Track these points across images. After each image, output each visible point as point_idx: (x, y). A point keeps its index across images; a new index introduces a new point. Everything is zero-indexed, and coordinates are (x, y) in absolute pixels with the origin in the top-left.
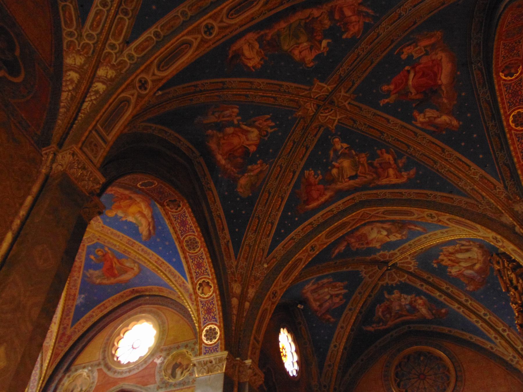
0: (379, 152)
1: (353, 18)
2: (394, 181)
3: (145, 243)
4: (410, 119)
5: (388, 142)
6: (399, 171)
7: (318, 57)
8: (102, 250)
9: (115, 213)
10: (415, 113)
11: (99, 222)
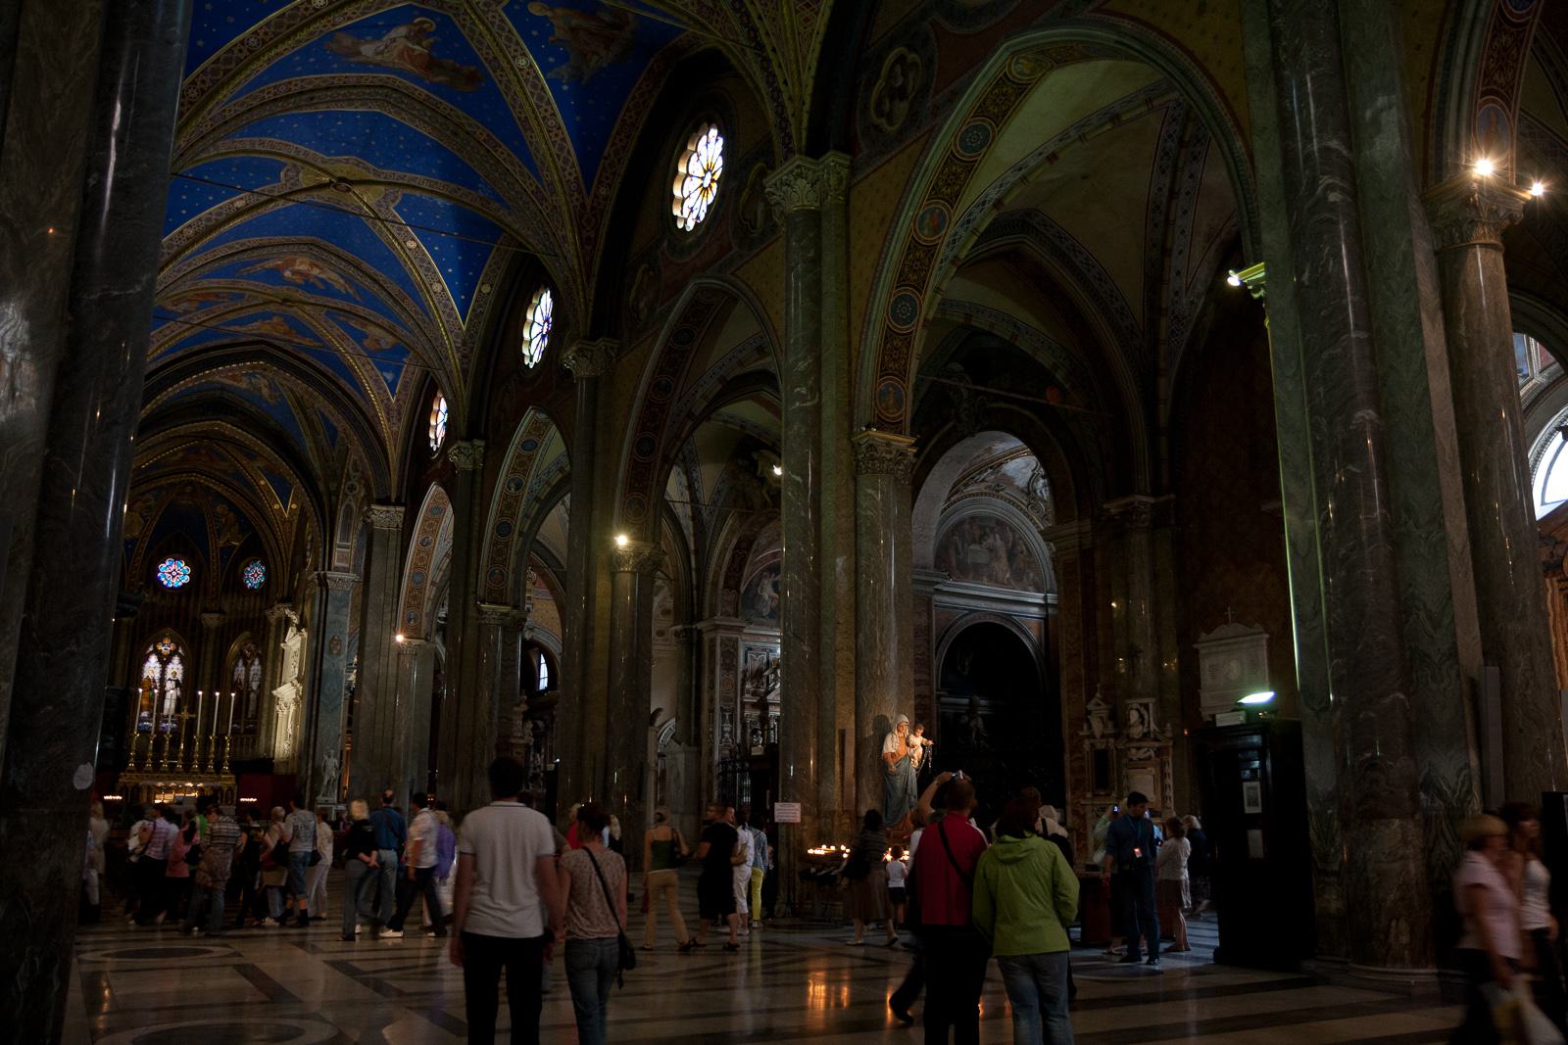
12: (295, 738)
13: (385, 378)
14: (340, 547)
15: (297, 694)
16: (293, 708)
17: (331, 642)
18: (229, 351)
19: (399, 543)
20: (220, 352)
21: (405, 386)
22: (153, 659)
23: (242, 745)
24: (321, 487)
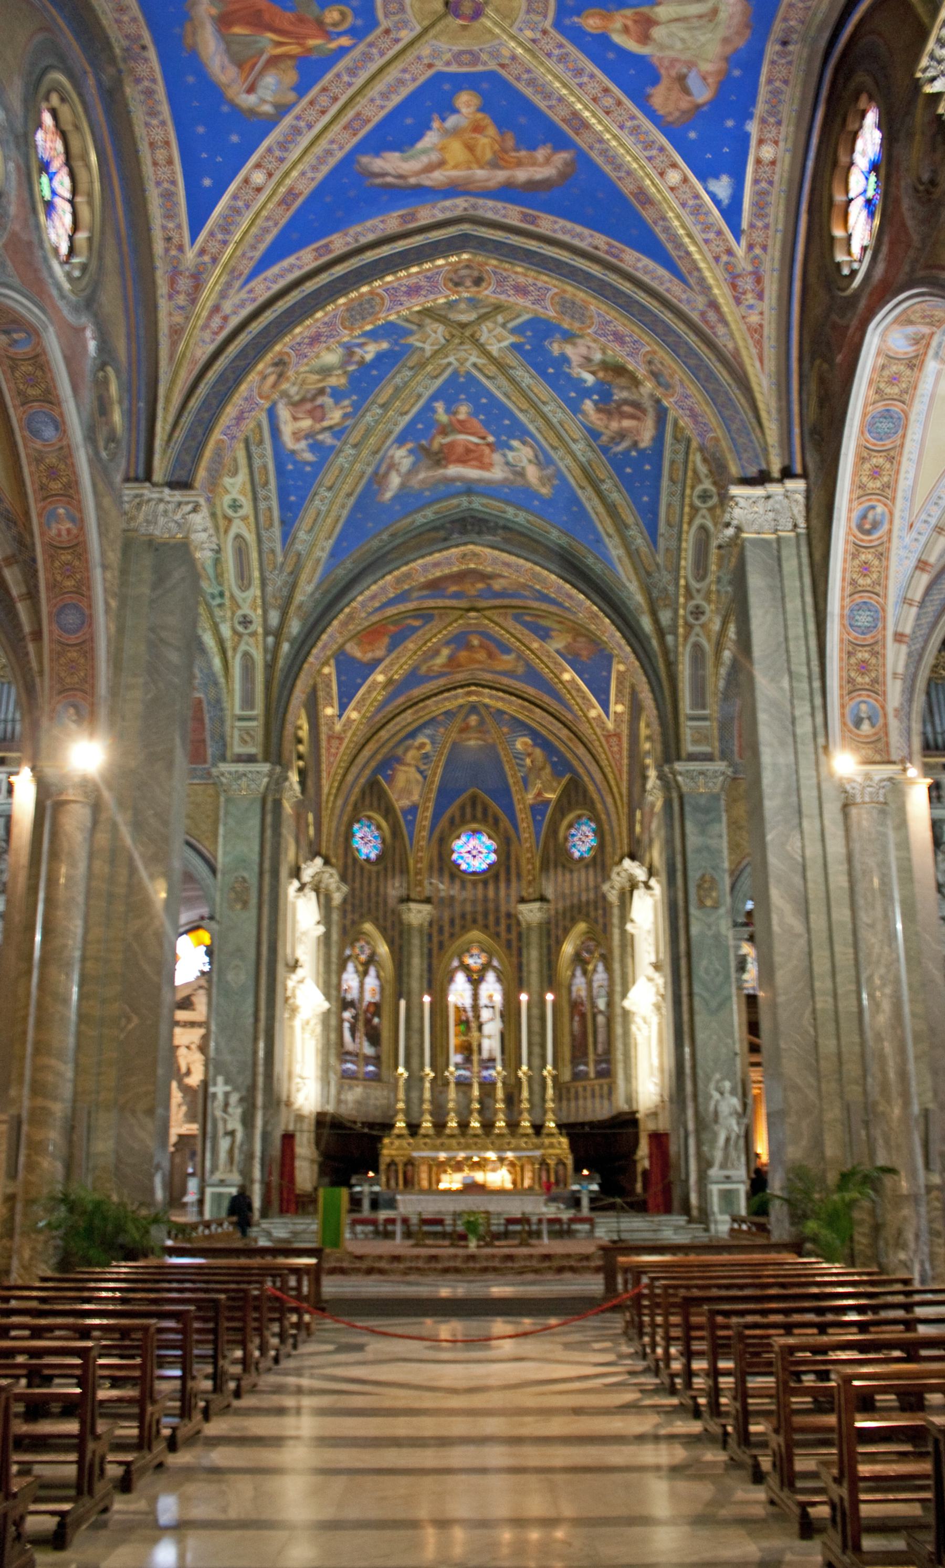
0: (346, 402)
1: (614, 425)
2: (287, 429)
3: (349, 160)
4: (401, 440)
5: (363, 416)
6: (310, 435)
7: (565, 359)
9: (464, 110)
10: (410, 445)
11: (448, 64)
12: (662, 1071)
14: (693, 718)
15: (658, 993)
16: (654, 1020)
17: (699, 887)
18: (401, 245)
19: (805, 560)
20: (385, 251)
21: (760, 207)
22: (460, 978)
23: (593, 1096)
24: (646, 623)
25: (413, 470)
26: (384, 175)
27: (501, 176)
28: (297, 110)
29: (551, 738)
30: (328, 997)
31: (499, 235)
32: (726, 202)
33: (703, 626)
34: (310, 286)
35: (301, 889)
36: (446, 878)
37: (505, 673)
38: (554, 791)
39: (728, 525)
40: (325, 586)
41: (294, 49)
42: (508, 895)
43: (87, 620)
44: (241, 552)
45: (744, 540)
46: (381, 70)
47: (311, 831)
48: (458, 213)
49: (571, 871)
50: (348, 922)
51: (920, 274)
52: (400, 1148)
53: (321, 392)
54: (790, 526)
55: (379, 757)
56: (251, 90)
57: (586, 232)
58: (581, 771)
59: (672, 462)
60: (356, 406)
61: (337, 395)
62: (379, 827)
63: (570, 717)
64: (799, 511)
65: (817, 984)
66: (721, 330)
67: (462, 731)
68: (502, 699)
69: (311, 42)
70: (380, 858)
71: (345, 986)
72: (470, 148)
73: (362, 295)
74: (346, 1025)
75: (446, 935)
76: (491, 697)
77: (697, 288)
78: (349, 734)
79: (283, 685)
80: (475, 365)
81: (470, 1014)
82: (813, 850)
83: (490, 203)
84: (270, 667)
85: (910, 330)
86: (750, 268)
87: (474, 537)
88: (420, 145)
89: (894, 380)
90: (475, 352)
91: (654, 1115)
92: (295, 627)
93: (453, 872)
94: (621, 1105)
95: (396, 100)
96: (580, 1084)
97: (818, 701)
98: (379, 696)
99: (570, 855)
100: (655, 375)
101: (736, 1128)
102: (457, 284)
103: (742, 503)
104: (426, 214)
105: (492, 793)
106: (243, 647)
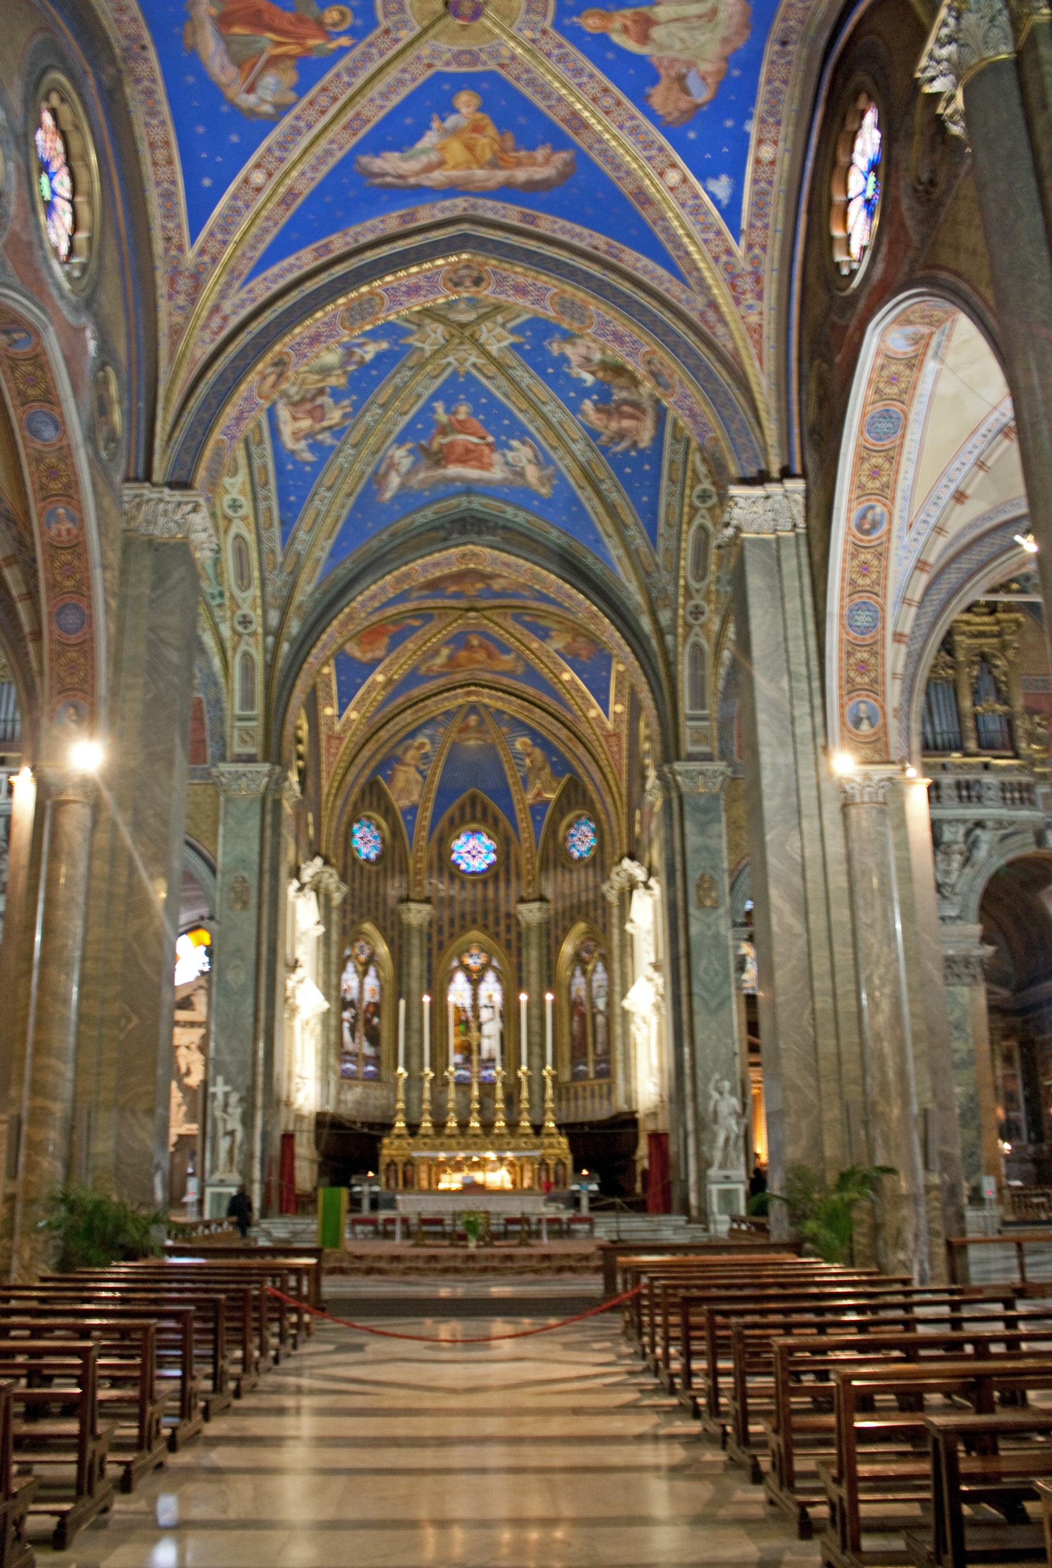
0: (346, 402)
1: (614, 425)
2: (287, 429)
3: (348, 160)
4: (400, 441)
6: (309, 435)
7: (564, 359)
8: (345, 26)
9: (464, 110)
10: (409, 445)
11: (448, 64)
12: (661, 1070)
13: (712, 196)
15: (657, 993)
16: (654, 1020)
17: (699, 887)
18: (401, 245)
19: (805, 560)
20: (385, 251)
21: (760, 206)
22: (460, 978)
23: (593, 1096)
24: (646, 623)
25: (413, 470)
26: (384, 175)
27: (500, 176)
28: (297, 110)
29: (550, 738)
30: (328, 997)
31: (498, 235)
32: (725, 202)
33: (702, 626)
34: (310, 286)
35: (301, 889)
36: (446, 879)
37: (504, 673)
38: (553, 791)
39: (727, 525)
40: (324, 587)
41: (293, 49)
42: (508, 896)
43: (87, 620)
44: (241, 552)
45: (744, 540)
46: (381, 70)
47: (311, 831)
48: (458, 213)
49: (571, 871)
50: (348, 922)
51: (920, 274)
52: (400, 1148)
53: (321, 392)
54: (789, 526)
55: (379, 757)
56: (251, 90)
57: (586, 232)
58: (580, 771)
59: (672, 462)
60: (356, 406)
61: (337, 395)
62: (378, 827)
63: (569, 717)
64: (798, 510)
65: (817, 984)
66: (720, 330)
67: (462, 730)
68: (501, 699)
69: (311, 42)
70: (380, 858)
71: (344, 986)
72: (470, 148)
73: (362, 295)
74: (346, 1025)
75: (446, 934)
76: (490, 697)
77: (696, 288)
78: (349, 734)
79: (282, 685)
80: (474, 365)
81: (470, 1014)
82: (812, 850)
83: (490, 203)
84: (269, 667)
85: (909, 330)
86: (749, 268)
87: (474, 537)
88: (420, 145)
89: (893, 380)
90: (475, 352)
91: (653, 1115)
92: (294, 627)
93: (453, 873)
94: (620, 1104)
95: (396, 100)
96: (579, 1084)
97: (817, 701)
98: (379, 696)
99: (570, 856)
100: (655, 375)
101: (735, 1128)
102: (456, 284)
103: (741, 502)
104: (426, 215)
105: (493, 793)
106: (242, 647)
